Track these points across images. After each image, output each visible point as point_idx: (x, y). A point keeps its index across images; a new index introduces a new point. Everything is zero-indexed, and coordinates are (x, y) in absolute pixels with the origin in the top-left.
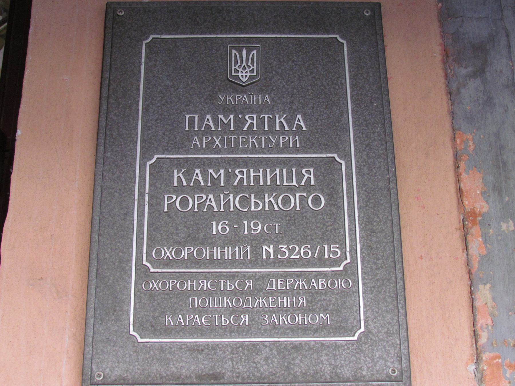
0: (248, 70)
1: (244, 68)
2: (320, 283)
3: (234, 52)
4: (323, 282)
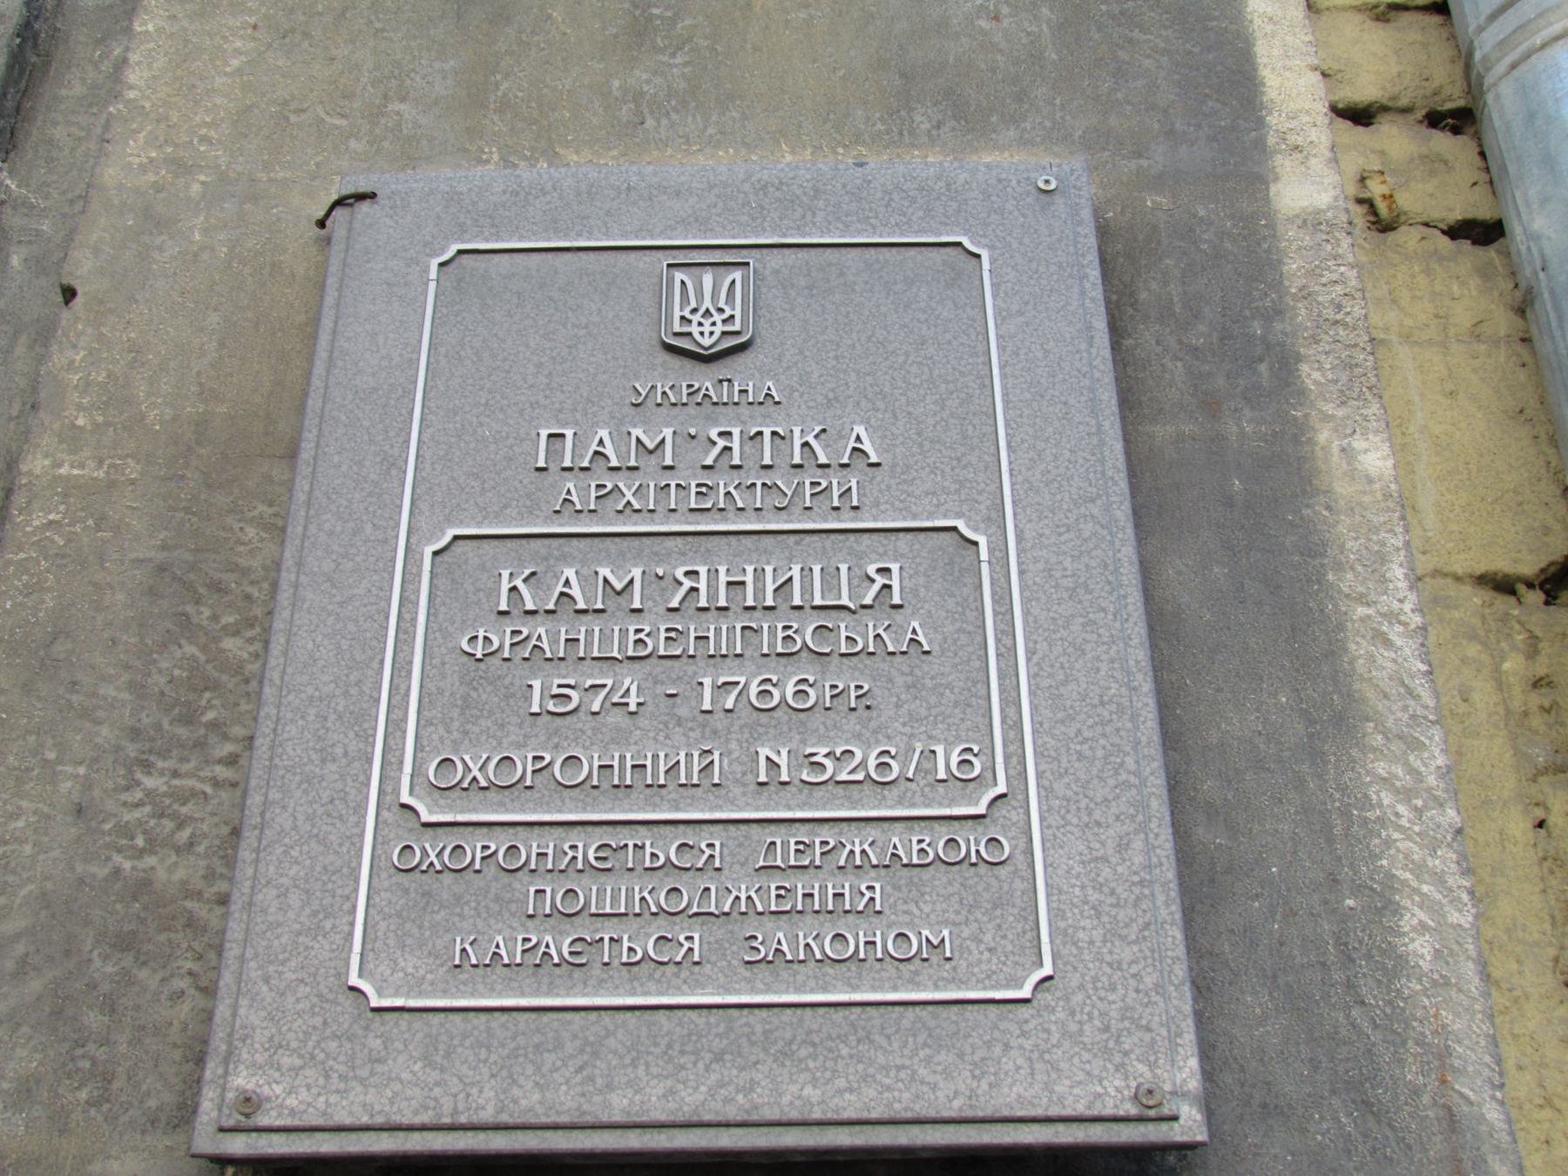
0: (718, 318)
2: (915, 847)
4: (924, 845)
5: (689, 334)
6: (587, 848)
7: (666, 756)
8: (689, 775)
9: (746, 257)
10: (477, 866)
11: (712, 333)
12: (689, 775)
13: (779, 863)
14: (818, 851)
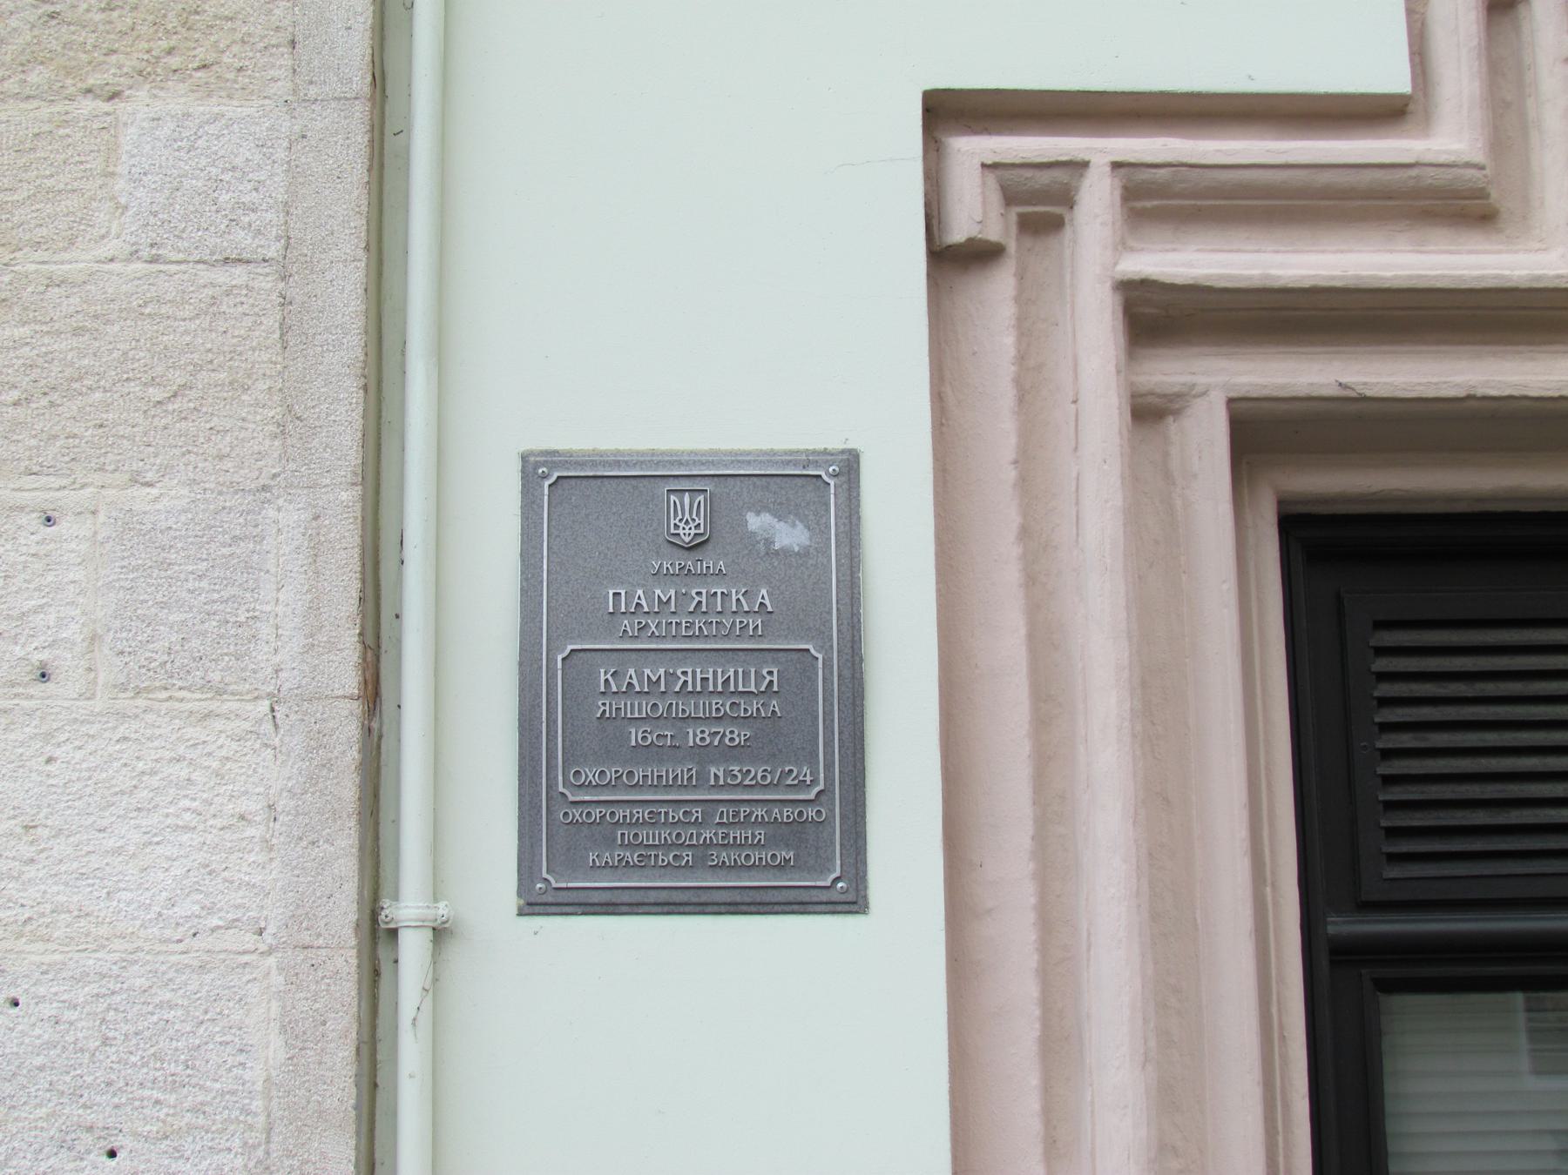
1: (687, 521)
2: (785, 814)
3: (673, 498)
5: (679, 534)
6: (643, 813)
7: (673, 771)
8: (682, 781)
9: (705, 485)
10: (598, 821)
11: (689, 534)
12: (682, 781)
13: (725, 820)
14: (742, 815)
